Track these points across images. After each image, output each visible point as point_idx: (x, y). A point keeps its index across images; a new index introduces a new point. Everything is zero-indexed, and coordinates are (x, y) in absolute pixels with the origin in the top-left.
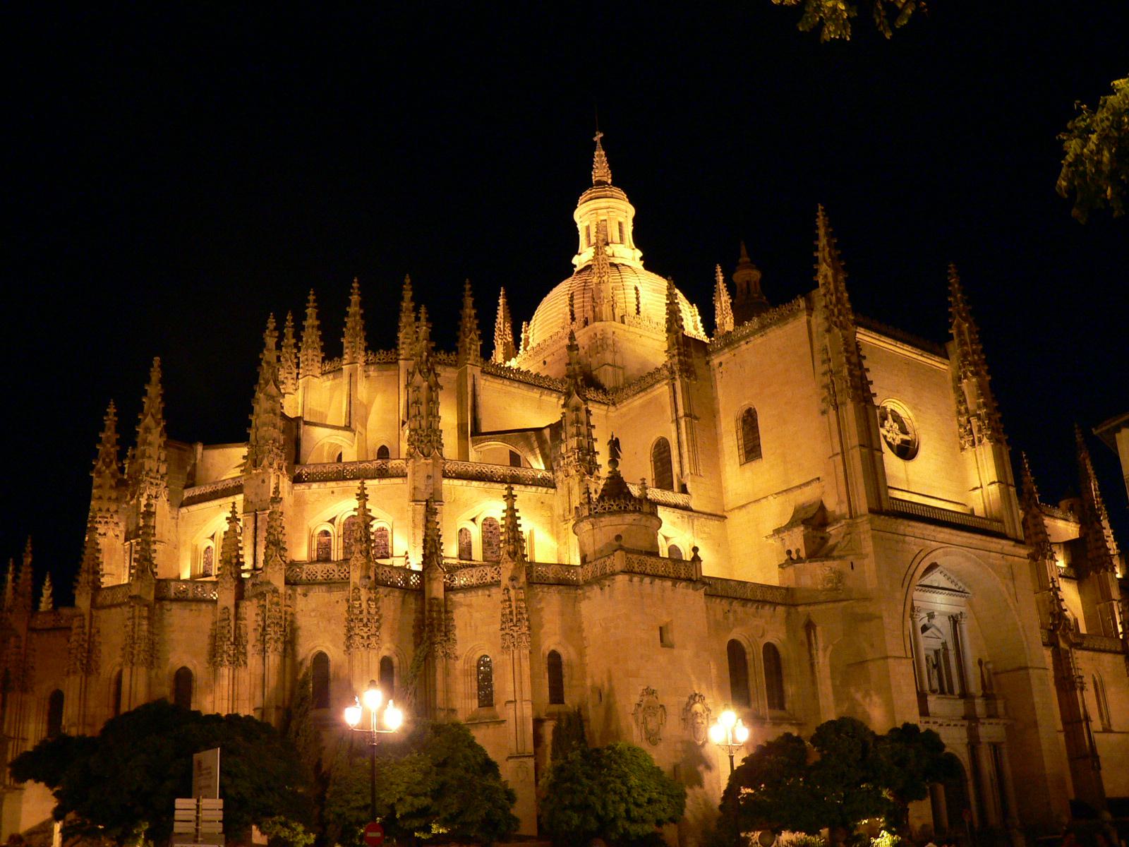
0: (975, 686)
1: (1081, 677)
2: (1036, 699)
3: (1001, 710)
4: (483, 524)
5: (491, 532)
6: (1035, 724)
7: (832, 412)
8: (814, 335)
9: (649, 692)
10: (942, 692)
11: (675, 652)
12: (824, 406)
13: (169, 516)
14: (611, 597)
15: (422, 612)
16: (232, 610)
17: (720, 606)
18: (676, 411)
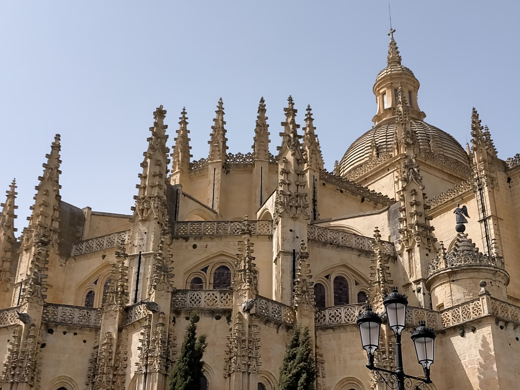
4: (335, 282)
5: (341, 290)
16: (115, 336)
18: (483, 211)
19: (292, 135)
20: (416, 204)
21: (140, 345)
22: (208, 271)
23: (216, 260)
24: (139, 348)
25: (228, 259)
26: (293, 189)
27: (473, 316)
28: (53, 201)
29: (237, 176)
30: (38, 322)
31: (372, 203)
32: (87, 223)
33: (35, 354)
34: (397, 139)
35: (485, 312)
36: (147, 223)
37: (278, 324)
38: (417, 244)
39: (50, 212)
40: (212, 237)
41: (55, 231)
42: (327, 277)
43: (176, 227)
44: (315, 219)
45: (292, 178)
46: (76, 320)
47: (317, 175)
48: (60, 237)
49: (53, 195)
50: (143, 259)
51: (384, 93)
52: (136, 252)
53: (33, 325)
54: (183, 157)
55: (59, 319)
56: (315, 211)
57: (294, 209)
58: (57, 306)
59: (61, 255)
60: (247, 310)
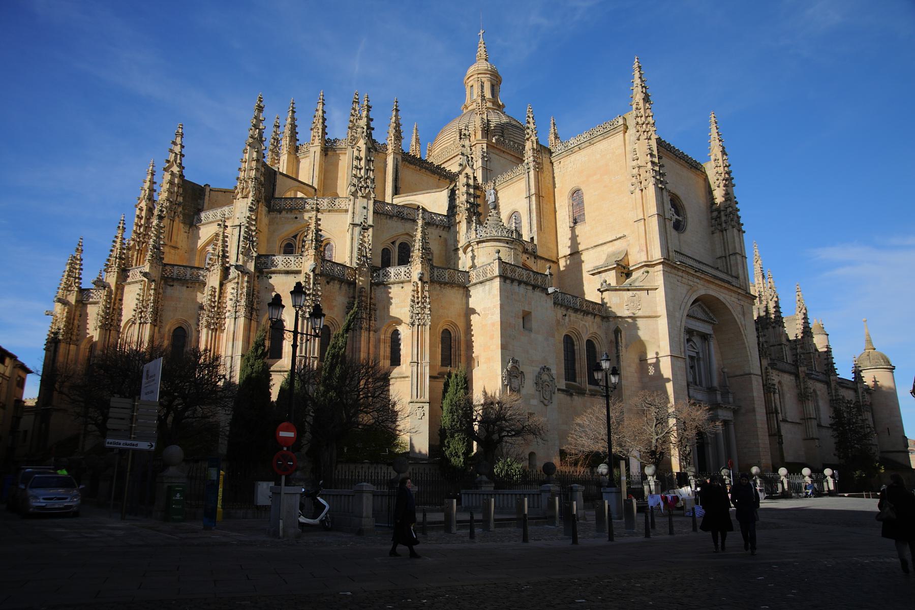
0: (716, 383)
1: (774, 385)
2: (755, 394)
3: (731, 400)
6: (754, 410)
7: (638, 191)
8: (627, 142)
9: (515, 362)
10: (696, 384)
11: (533, 335)
12: (632, 188)
13: (183, 230)
14: (489, 292)
15: (354, 298)
16: (217, 290)
17: (560, 312)
20: (468, 185)
21: (231, 297)
24: (231, 300)
27: (489, 276)
32: (207, 197)
35: (497, 273)
37: (342, 281)
38: (464, 217)
41: (179, 204)
42: (393, 243)
47: (400, 158)
54: (290, 141)
58: (173, 266)
59: (184, 223)
60: (313, 271)
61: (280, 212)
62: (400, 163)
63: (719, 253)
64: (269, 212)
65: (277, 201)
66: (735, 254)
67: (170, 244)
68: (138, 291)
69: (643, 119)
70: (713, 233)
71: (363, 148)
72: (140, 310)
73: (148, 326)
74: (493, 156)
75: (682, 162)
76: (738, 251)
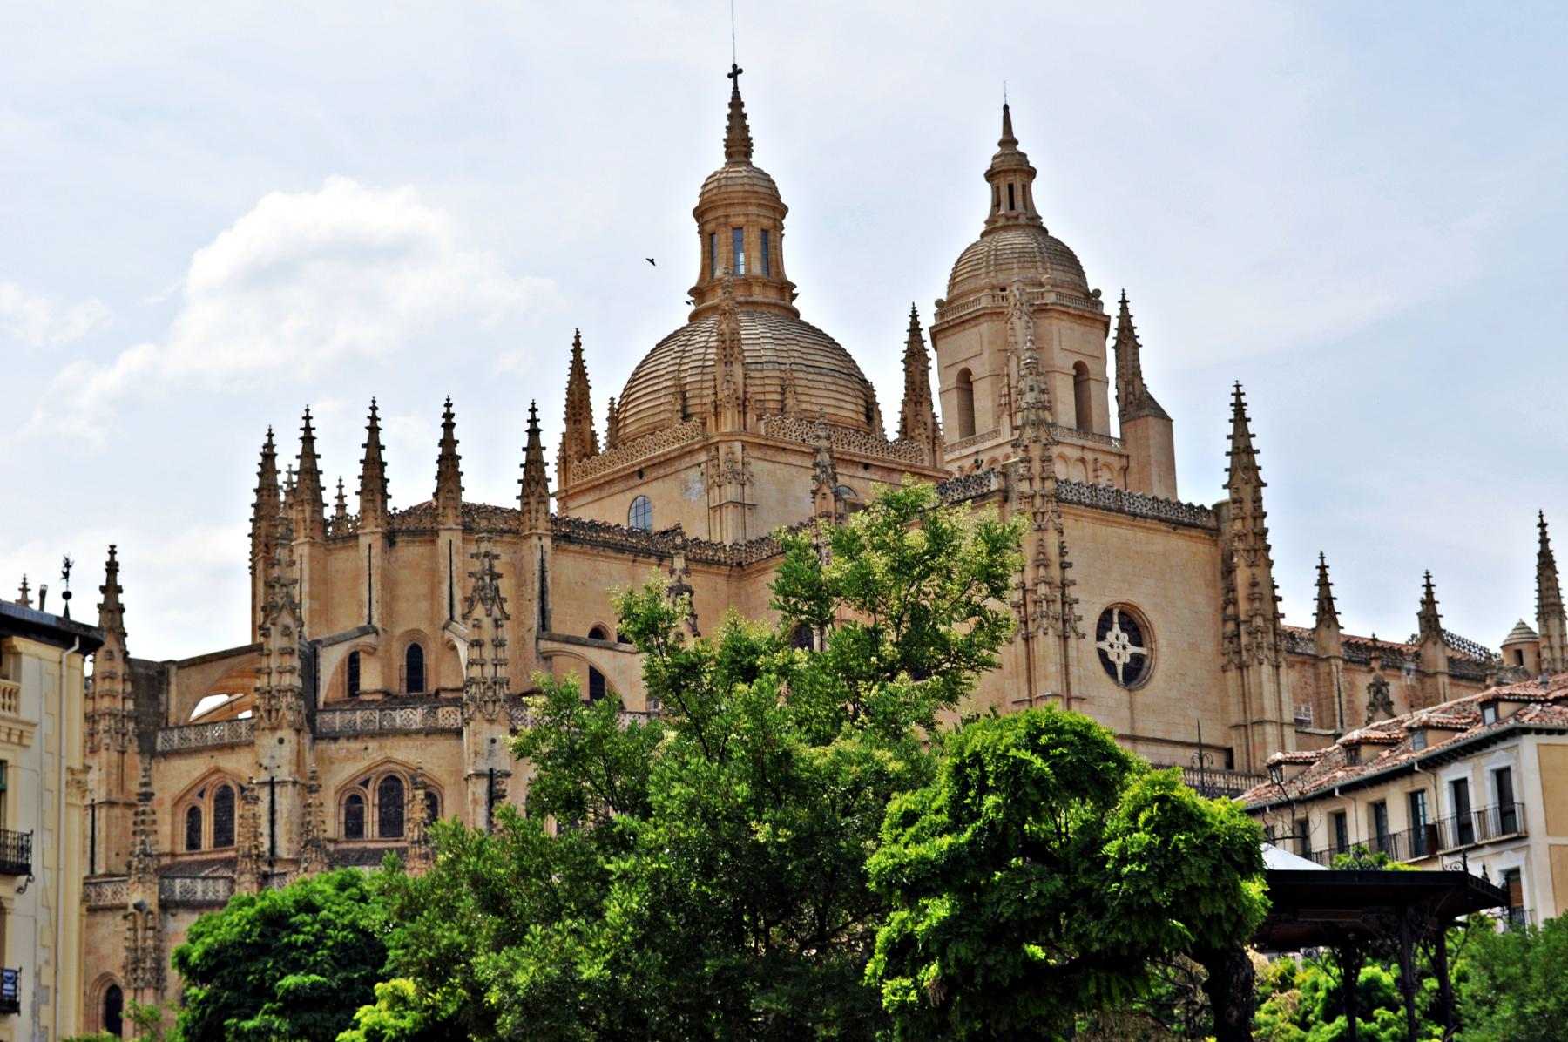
7: (1019, 639)
13: (140, 766)
19: (487, 579)
22: (371, 786)
23: (381, 769)
25: (398, 768)
26: (489, 671)
28: (120, 668)
29: (409, 552)
30: (154, 907)
31: (653, 560)
32: (173, 688)
33: (157, 948)
34: (716, 394)
36: (279, 734)
39: (119, 687)
40: (373, 735)
41: (129, 717)
43: (318, 719)
44: (544, 626)
45: (488, 652)
46: (199, 896)
47: (547, 542)
48: (137, 724)
49: (118, 656)
50: (277, 789)
51: (712, 235)
52: (265, 777)
53: (150, 913)
54: (314, 512)
55: (178, 896)
56: (544, 612)
57: (490, 706)
59: (142, 752)
61: (335, 739)
62: (548, 557)
63: (1235, 717)
64: (314, 740)
65: (327, 717)
66: (1262, 722)
67: (122, 799)
68: (128, 934)
69: (1037, 485)
70: (1224, 670)
71: (487, 623)
72: (134, 965)
73: (149, 993)
74: (758, 467)
75: (1149, 523)
76: (1270, 714)
